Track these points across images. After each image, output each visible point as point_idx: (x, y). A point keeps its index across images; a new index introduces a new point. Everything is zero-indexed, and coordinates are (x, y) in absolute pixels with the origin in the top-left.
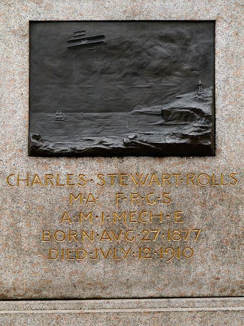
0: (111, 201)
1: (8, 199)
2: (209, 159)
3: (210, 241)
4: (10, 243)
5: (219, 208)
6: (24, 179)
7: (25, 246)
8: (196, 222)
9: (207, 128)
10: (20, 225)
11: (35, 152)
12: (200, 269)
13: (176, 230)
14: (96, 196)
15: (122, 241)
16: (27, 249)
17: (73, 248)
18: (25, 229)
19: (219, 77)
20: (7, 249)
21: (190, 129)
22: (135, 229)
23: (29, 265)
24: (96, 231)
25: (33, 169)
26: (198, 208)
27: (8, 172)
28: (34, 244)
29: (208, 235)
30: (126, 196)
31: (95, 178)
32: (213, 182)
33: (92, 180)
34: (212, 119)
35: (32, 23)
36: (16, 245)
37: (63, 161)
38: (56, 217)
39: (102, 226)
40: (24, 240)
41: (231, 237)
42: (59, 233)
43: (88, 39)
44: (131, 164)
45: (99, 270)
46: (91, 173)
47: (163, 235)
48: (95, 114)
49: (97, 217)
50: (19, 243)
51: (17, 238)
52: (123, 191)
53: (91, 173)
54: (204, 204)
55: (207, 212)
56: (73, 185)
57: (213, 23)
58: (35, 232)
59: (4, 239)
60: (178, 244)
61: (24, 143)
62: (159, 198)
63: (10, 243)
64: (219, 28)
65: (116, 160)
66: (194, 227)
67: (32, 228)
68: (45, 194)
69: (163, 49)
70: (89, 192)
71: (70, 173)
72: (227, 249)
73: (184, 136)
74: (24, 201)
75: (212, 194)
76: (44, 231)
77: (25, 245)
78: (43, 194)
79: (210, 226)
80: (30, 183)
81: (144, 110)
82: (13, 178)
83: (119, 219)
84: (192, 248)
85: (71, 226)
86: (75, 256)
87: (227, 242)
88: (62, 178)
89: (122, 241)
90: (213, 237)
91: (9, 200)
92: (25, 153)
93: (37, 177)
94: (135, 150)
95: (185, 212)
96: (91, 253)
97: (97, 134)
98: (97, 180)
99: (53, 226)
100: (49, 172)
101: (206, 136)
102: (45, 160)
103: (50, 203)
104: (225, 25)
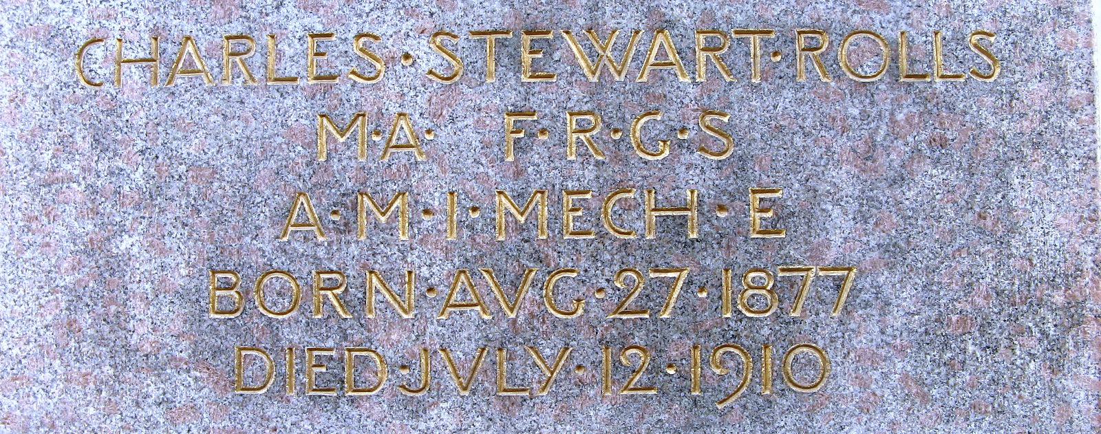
0: (486, 145)
1: (78, 138)
3: (896, 320)
4: (85, 319)
5: (929, 176)
6: (141, 55)
7: (141, 334)
10: (123, 247)
13: (757, 270)
14: (426, 123)
15: (532, 315)
16: (147, 348)
17: (330, 343)
18: (144, 265)
20: (73, 344)
22: (584, 263)
23: (157, 413)
24: (425, 271)
25: (176, 16)
26: (842, 176)
27: (83, 32)
28: (178, 326)
29: (887, 290)
30: (546, 123)
31: (422, 48)
33: (407, 56)
36: (106, 328)
38: (262, 216)
39: (447, 251)
40: (137, 307)
41: (980, 301)
42: (275, 282)
46: (405, 27)
47: (702, 290)
49: (426, 212)
50: (118, 322)
51: (113, 301)
52: (534, 102)
53: (405, 27)
55: (883, 193)
56: (333, 77)
58: (179, 277)
59: (63, 305)
60: (766, 331)
62: (683, 130)
63: (85, 319)
66: (831, 256)
67: (168, 260)
68: (220, 119)
70: (394, 110)
71: (319, 28)
72: (964, 351)
74: (140, 145)
75: (900, 117)
76: (214, 272)
77: (141, 330)
78: (213, 118)
79: (893, 253)
80: (162, 71)
82: (97, 51)
83: (516, 222)
84: (820, 345)
85: (321, 253)
87: (963, 321)
88: (289, 52)
89: (532, 315)
90: (907, 298)
91: (83, 143)
93: (190, 48)
95: (789, 193)
96: (403, 367)
98: (428, 57)
99: (250, 252)
100: (237, 28)
103: (240, 157)
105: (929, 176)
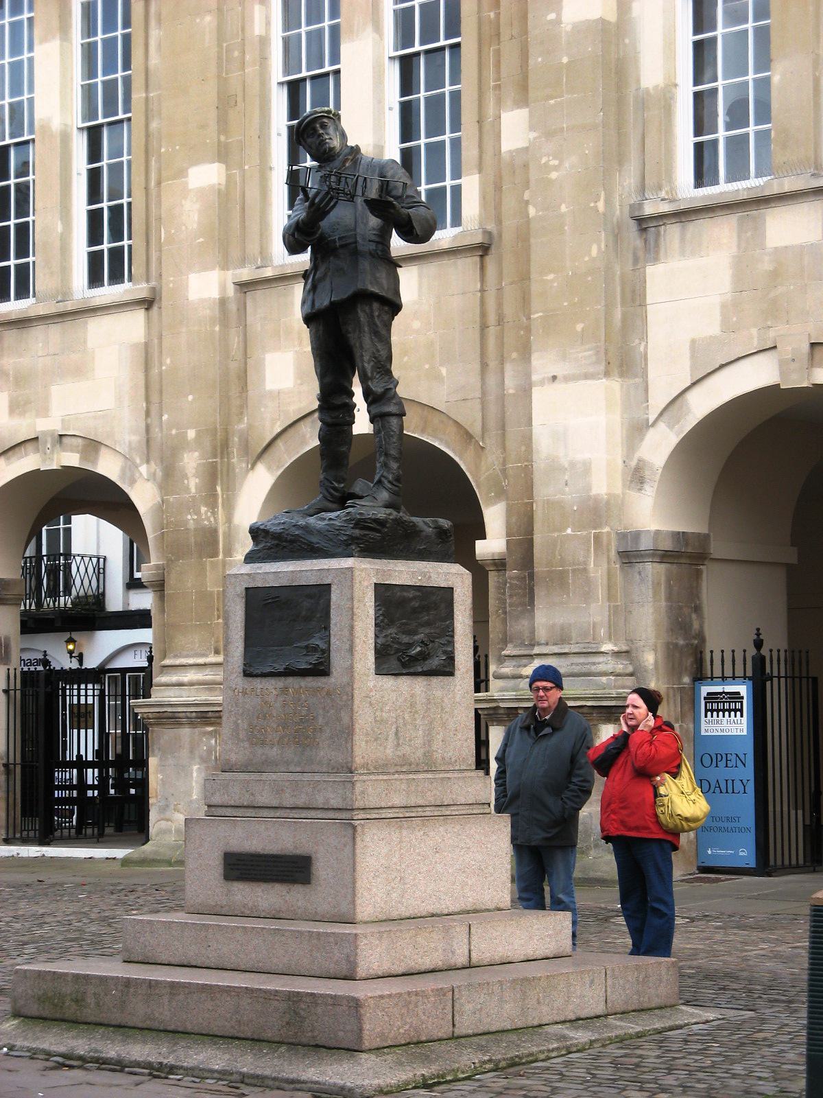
2: (327, 677)
3: (327, 734)
5: (332, 711)
7: (241, 736)
8: (321, 721)
9: (321, 658)
11: (247, 674)
12: (322, 753)
18: (241, 725)
19: (333, 622)
21: (313, 659)
23: (242, 749)
32: (329, 694)
34: (326, 652)
35: (246, 588)
37: (258, 680)
43: (273, 598)
44: (290, 680)
45: (274, 752)
48: (276, 648)
54: (324, 708)
57: (329, 585)
61: (240, 670)
64: (333, 588)
65: (283, 678)
69: (306, 604)
73: (311, 664)
81: (299, 645)
86: (263, 743)
92: (242, 674)
94: (289, 673)
97: (274, 662)
98: (275, 692)
101: (321, 663)
102: (251, 679)
104: (335, 587)
105: (332, 711)
